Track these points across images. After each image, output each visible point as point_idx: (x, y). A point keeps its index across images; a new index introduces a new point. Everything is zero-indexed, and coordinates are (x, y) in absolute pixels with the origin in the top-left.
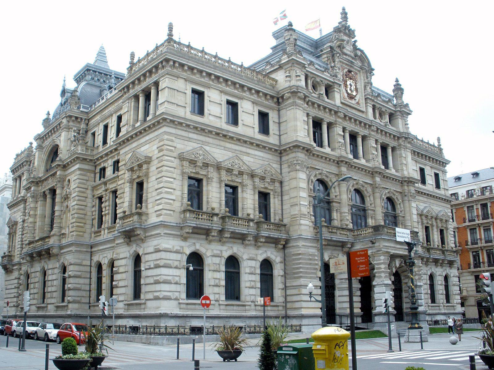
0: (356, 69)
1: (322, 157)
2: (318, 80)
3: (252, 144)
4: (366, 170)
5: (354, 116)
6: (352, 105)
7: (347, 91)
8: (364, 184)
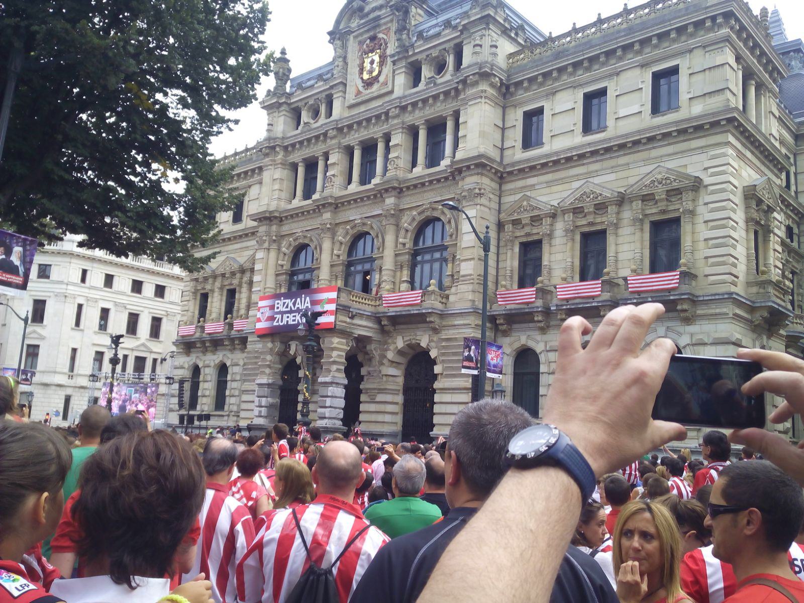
0: (385, 24)
1: (297, 214)
2: (311, 102)
3: (247, 235)
4: (368, 197)
5: (353, 119)
6: (375, 94)
7: (362, 78)
8: (365, 221)
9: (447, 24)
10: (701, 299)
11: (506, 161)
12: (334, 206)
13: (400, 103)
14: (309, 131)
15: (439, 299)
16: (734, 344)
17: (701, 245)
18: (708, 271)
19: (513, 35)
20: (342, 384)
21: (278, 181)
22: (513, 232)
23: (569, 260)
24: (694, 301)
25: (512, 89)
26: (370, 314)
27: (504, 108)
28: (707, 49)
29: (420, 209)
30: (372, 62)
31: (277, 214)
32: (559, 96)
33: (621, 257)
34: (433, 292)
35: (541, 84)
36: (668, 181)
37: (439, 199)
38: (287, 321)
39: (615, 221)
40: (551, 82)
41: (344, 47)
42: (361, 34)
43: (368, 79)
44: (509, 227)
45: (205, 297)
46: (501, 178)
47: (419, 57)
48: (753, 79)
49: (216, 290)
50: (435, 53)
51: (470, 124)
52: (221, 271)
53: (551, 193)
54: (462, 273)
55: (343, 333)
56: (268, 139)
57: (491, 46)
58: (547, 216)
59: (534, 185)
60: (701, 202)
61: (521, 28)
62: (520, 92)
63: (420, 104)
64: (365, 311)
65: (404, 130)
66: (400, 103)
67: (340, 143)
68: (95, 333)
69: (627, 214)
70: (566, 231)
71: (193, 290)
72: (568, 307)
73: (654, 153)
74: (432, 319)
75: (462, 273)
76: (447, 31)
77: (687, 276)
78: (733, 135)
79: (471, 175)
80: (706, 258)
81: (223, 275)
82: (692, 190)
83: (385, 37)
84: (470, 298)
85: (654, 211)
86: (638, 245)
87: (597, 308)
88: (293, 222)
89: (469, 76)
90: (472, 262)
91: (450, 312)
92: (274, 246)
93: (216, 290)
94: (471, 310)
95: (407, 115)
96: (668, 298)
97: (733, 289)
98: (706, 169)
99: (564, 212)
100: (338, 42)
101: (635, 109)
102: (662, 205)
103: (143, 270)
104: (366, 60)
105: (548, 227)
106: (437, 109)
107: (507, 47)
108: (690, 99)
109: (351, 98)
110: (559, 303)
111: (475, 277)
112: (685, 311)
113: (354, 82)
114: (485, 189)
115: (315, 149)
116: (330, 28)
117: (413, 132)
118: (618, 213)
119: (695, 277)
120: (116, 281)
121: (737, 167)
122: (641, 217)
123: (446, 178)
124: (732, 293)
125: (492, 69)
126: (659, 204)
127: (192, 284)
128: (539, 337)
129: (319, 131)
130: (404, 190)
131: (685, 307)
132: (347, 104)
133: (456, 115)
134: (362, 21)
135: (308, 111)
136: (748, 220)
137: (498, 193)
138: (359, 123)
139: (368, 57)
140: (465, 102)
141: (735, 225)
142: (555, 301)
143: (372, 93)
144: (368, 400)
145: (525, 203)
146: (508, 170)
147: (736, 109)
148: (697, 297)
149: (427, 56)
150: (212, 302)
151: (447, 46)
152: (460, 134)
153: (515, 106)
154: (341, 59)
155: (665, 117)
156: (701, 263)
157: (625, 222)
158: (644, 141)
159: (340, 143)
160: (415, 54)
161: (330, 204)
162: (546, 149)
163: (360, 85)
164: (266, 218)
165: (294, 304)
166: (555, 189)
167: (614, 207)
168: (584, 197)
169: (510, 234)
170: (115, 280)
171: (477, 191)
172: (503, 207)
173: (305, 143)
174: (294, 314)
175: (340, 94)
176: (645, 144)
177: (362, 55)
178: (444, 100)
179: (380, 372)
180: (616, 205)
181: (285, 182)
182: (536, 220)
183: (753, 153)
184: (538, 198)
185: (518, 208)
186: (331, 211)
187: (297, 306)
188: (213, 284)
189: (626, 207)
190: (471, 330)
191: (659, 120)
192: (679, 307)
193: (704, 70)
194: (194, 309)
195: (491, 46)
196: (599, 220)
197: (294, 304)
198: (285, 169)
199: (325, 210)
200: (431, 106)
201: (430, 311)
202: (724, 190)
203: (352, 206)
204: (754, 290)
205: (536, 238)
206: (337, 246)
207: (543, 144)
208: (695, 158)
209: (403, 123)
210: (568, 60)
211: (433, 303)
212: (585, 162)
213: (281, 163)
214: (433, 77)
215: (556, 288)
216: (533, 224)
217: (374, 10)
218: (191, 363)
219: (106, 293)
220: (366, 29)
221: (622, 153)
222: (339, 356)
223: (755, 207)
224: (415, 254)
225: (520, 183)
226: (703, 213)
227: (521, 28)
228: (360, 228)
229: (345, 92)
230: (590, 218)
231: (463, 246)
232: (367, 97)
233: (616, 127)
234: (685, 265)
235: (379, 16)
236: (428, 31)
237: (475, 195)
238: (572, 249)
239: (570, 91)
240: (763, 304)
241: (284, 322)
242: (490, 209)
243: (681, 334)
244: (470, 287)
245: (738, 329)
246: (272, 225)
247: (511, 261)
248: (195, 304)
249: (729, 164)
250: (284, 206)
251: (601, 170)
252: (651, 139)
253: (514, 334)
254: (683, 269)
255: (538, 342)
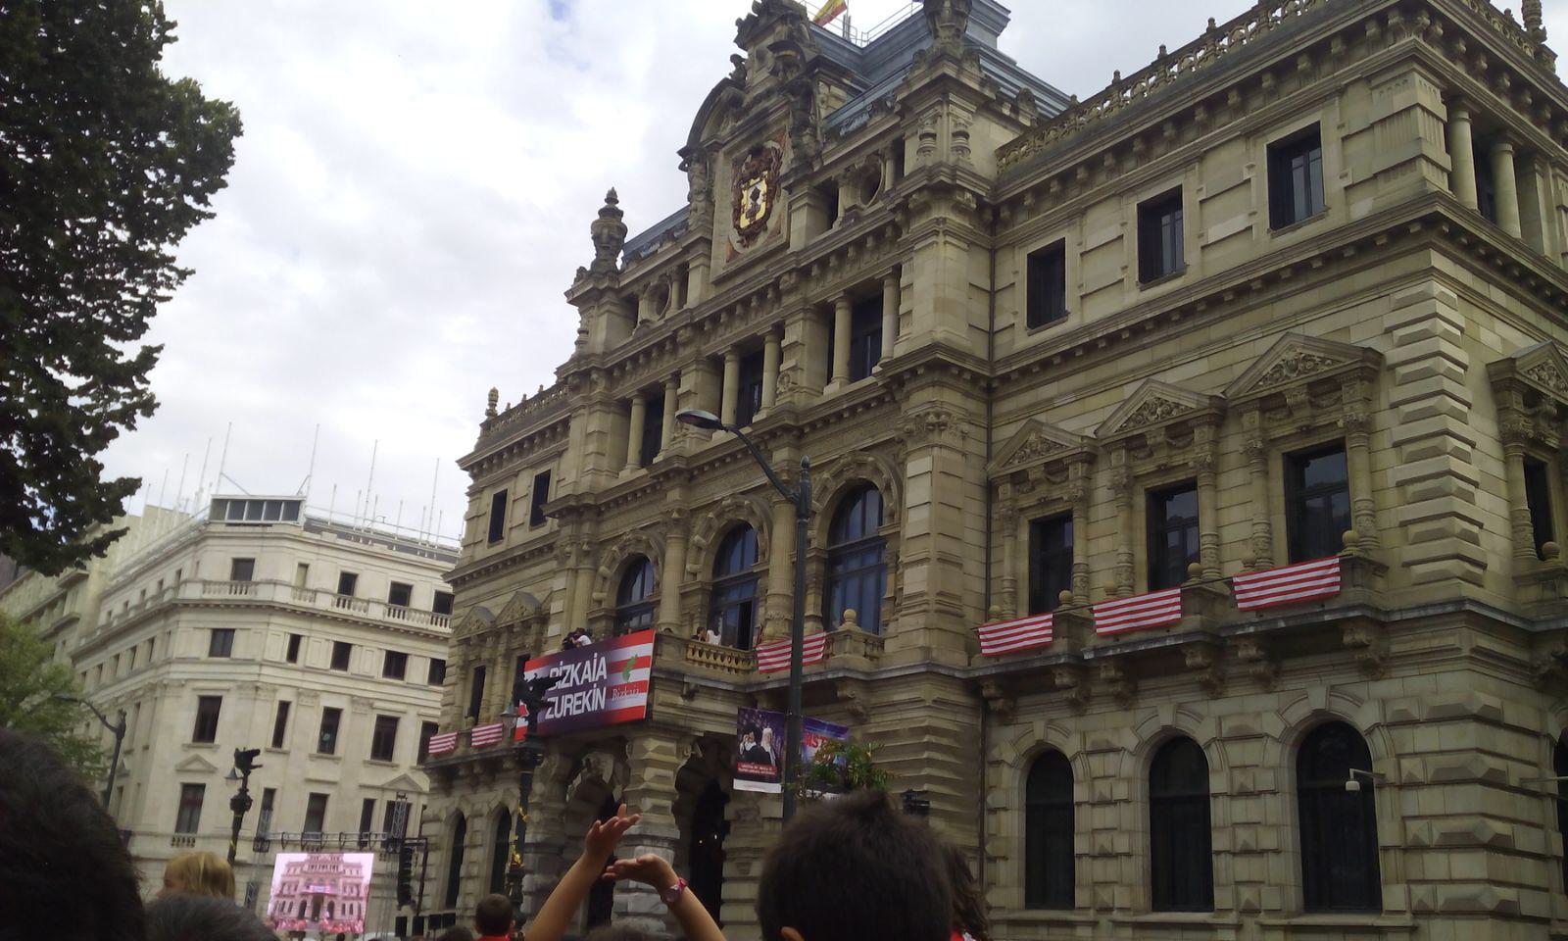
0: (778, 121)
2: (654, 282)
5: (718, 305)
6: (758, 254)
7: (737, 227)
9: (879, 106)
10: (1397, 617)
11: (1000, 354)
12: (686, 475)
13: (798, 262)
14: (646, 335)
15: (862, 647)
16: (1478, 718)
17: (1392, 497)
18: (1411, 553)
19: (1006, 112)
20: (665, 839)
21: (594, 437)
22: (1016, 500)
23: (1123, 549)
24: (1382, 624)
25: (1005, 214)
26: (730, 688)
27: (993, 253)
28: (1375, 82)
29: (835, 468)
30: (755, 196)
31: (590, 501)
32: (1095, 216)
33: (1228, 535)
34: (848, 634)
35: (1059, 197)
36: (1309, 364)
37: (868, 442)
38: (568, 709)
39: (1209, 459)
40: (1075, 192)
41: (708, 174)
42: (737, 147)
43: (749, 226)
44: (1005, 490)
45: (480, 673)
46: (989, 390)
47: (833, 174)
48: (1506, 140)
49: (500, 659)
50: (859, 162)
51: (917, 287)
52: (506, 620)
53: (1080, 413)
54: (907, 591)
55: (669, 730)
56: (575, 359)
57: (956, 135)
58: (1076, 458)
59: (1051, 400)
60: (1384, 403)
61: (1026, 97)
62: (1021, 217)
63: (833, 262)
64: (718, 681)
65: (809, 315)
66: (798, 262)
67: (699, 352)
68: (311, 757)
69: (1234, 443)
70: (1114, 487)
71: (461, 663)
72: (1118, 651)
73: (1282, 309)
74: (847, 692)
75: (907, 591)
76: (878, 118)
77: (1362, 567)
78: (1444, 253)
79: (922, 388)
80: (1404, 524)
81: (510, 628)
82: (1362, 379)
83: (777, 146)
84: (921, 642)
85: (1288, 430)
86: (1259, 506)
87: (1176, 650)
88: (620, 514)
89: (910, 195)
90: (925, 567)
91: (884, 676)
92: (587, 564)
93: (500, 659)
94: (923, 670)
95: (812, 285)
96: (1315, 620)
97: (1469, 590)
98: (1389, 331)
99: (1110, 447)
100: (697, 167)
101: (1239, 223)
102: (1303, 416)
103: (407, 632)
104: (745, 193)
105: (1079, 483)
106: (864, 267)
107: (989, 137)
108: (1346, 189)
109: (720, 264)
110: (1100, 643)
111: (932, 598)
112: (1362, 646)
113: (725, 236)
114: (948, 415)
115: (659, 369)
116: (683, 143)
117: (824, 315)
118: (1216, 442)
119: (1381, 569)
120: (355, 656)
121: (1461, 321)
122: (1259, 445)
123: (880, 400)
124: (1461, 601)
125: (954, 177)
126: (1297, 415)
127: (463, 648)
128: (1071, 723)
129: (663, 334)
130: (807, 430)
131: (1361, 636)
132: (712, 278)
133: (897, 271)
134: (739, 123)
135: (651, 299)
136: (1507, 438)
137: (984, 422)
138: (730, 310)
139: (749, 187)
140: (909, 250)
141: (1468, 448)
142: (1092, 641)
143: (757, 250)
144: (738, 875)
145: (1032, 437)
146: (999, 373)
147: (1438, 196)
148: (1387, 613)
149: (847, 170)
150: (492, 684)
151: (880, 146)
152: (902, 310)
153: (1012, 246)
154: (701, 197)
155: (1299, 232)
156: (1393, 538)
157: (1233, 460)
158: (1256, 285)
159: (699, 352)
160: (824, 169)
161: (678, 471)
162: (1072, 323)
163: (735, 236)
164: (571, 510)
165: (580, 673)
166: (1093, 402)
167: (1206, 429)
168: (1145, 413)
169: (1008, 503)
170: (354, 654)
171: (932, 419)
172: (996, 448)
173: (641, 360)
174: (580, 694)
175: (701, 260)
176: (1260, 291)
177: (739, 184)
178: (877, 248)
179: (758, 811)
180: (1210, 424)
181: (609, 439)
182: (1056, 469)
183: (1509, 292)
184: (1062, 425)
185: (1021, 448)
186: (681, 486)
187: (584, 677)
188: (495, 648)
189: (1232, 428)
190: (923, 713)
191: (1287, 239)
192: (1347, 639)
193: (1372, 126)
194: (463, 701)
195: (956, 135)
196: (1178, 460)
197: (580, 673)
198: (609, 413)
199: (671, 484)
200: (855, 261)
201: (841, 675)
202: (1429, 373)
203: (717, 473)
204: (1532, 593)
205: (1059, 508)
206: (692, 554)
207: (1067, 314)
208: (1366, 311)
209: (805, 300)
210: (1102, 143)
211: (852, 659)
212: (1146, 340)
213: (601, 403)
214: (855, 207)
215: (1092, 611)
216: (1052, 478)
217: (758, 100)
218: (452, 809)
219: (337, 680)
220: (744, 136)
221: (1216, 315)
222: (659, 778)
223: (1520, 408)
224: (832, 560)
225: (1026, 399)
226: (1392, 427)
227: (1026, 97)
228: (731, 516)
229: (709, 257)
230: (1161, 457)
231: (908, 536)
232: (745, 261)
233: (1203, 265)
234: (1355, 543)
235: (766, 109)
236: (848, 125)
237: (930, 427)
238: (1130, 527)
239: (1113, 203)
240: (1553, 626)
241: (564, 712)
242: (964, 455)
243: (1362, 701)
244: (921, 620)
245: (1492, 684)
246: (581, 523)
247: (1015, 561)
248: (464, 690)
249: (1436, 315)
250: (605, 482)
251: (1180, 354)
252: (1271, 280)
253: (1021, 719)
254: (1351, 550)
255: (1067, 734)
